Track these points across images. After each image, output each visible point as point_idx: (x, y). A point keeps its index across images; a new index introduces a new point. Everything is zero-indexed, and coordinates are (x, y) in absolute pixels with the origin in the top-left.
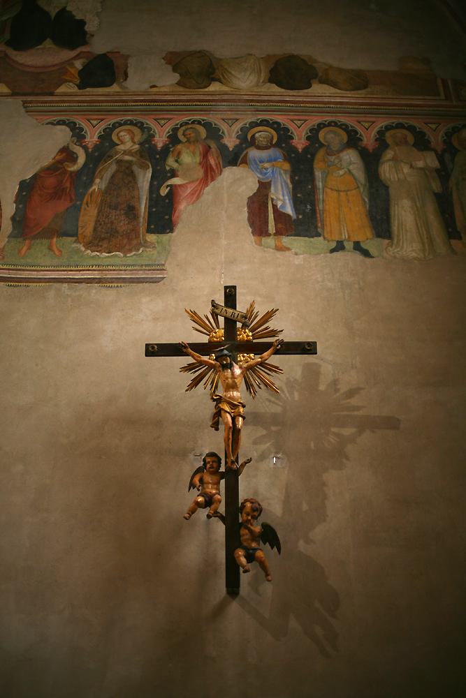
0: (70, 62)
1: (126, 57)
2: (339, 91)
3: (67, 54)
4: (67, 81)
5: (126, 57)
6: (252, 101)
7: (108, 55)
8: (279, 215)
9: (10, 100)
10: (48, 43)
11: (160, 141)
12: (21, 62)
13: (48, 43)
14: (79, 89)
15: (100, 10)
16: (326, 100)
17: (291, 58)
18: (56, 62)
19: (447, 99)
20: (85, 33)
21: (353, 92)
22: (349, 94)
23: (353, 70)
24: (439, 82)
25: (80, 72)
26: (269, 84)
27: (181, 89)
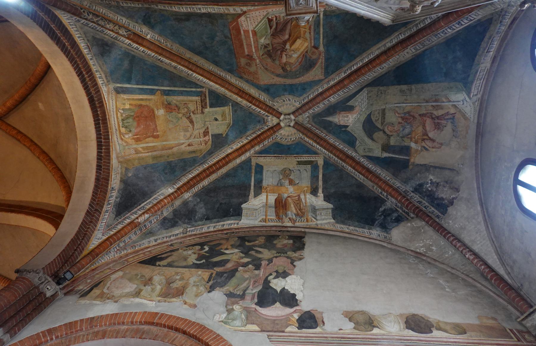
0: (291, 314)
1: (322, 313)
2: (451, 335)
3: (288, 310)
4: (291, 325)
5: (322, 313)
6: (401, 340)
7: (312, 312)
9: (260, 334)
10: (278, 304)
12: (264, 314)
13: (278, 304)
14: (299, 329)
15: (302, 289)
16: (445, 340)
17: (414, 315)
18: (283, 314)
19: (519, 340)
20: (297, 300)
21: (459, 336)
22: (458, 337)
23: (453, 323)
24: (509, 331)
25: (297, 320)
26: (407, 330)
27: (357, 331)
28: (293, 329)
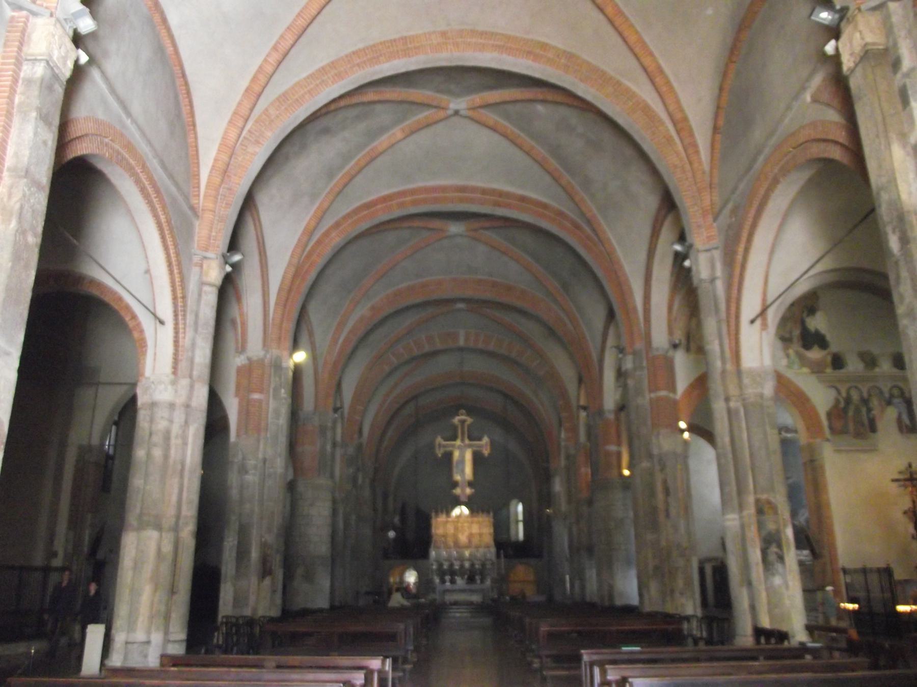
8: (907, 426)
11: (865, 395)
28: (829, 370)
